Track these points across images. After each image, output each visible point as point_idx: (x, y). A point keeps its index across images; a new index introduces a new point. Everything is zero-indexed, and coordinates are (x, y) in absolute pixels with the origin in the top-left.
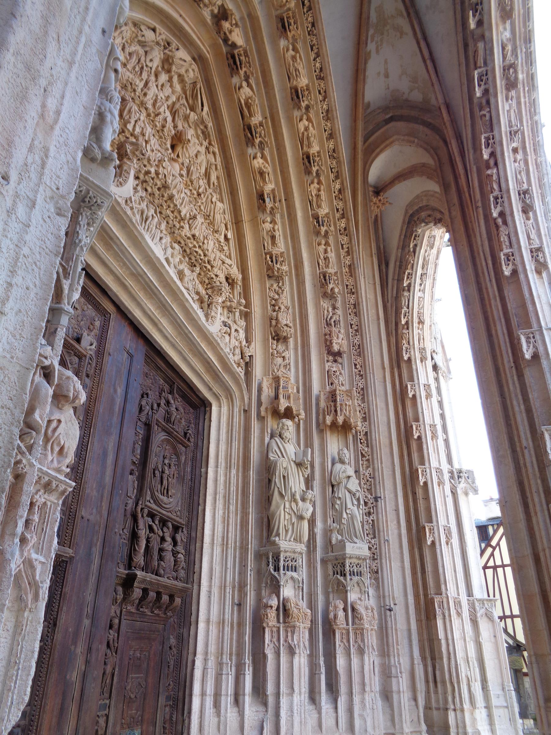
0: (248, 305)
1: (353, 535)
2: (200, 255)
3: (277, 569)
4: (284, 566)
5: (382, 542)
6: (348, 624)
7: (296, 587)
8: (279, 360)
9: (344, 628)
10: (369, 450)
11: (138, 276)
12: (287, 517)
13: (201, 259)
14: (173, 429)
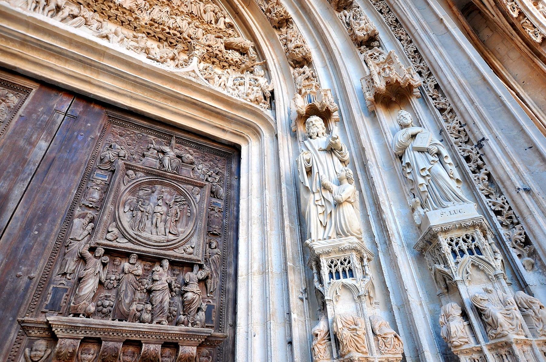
0: (263, 57)
1: (443, 199)
2: (175, 35)
3: (321, 281)
4: (331, 273)
5: (514, 193)
6: (478, 342)
7: (356, 298)
9: (472, 350)
10: (448, 99)
11: (24, 42)
12: (321, 210)
13: (180, 38)
14: (165, 171)
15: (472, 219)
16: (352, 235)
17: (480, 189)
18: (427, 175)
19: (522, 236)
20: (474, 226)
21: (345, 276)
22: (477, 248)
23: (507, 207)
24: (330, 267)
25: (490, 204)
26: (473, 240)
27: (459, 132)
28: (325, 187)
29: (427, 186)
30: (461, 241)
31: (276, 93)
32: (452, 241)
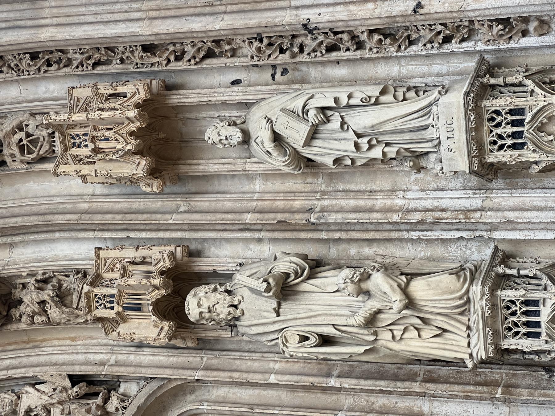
4: (529, 335)
8: (54, 313)
15: (466, 112)
16: (468, 291)
17: (397, 52)
18: (369, 142)
19: (494, 26)
20: (477, 110)
21: (537, 313)
22: (512, 112)
23: (440, 28)
24: (517, 333)
25: (429, 46)
26: (498, 113)
27: (270, 45)
28: (371, 321)
29: (387, 145)
30: (499, 131)
31: (78, 370)
32: (495, 143)
